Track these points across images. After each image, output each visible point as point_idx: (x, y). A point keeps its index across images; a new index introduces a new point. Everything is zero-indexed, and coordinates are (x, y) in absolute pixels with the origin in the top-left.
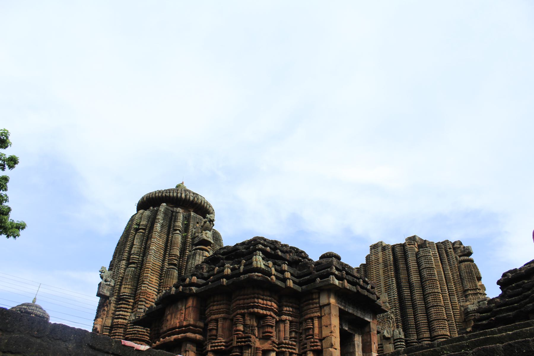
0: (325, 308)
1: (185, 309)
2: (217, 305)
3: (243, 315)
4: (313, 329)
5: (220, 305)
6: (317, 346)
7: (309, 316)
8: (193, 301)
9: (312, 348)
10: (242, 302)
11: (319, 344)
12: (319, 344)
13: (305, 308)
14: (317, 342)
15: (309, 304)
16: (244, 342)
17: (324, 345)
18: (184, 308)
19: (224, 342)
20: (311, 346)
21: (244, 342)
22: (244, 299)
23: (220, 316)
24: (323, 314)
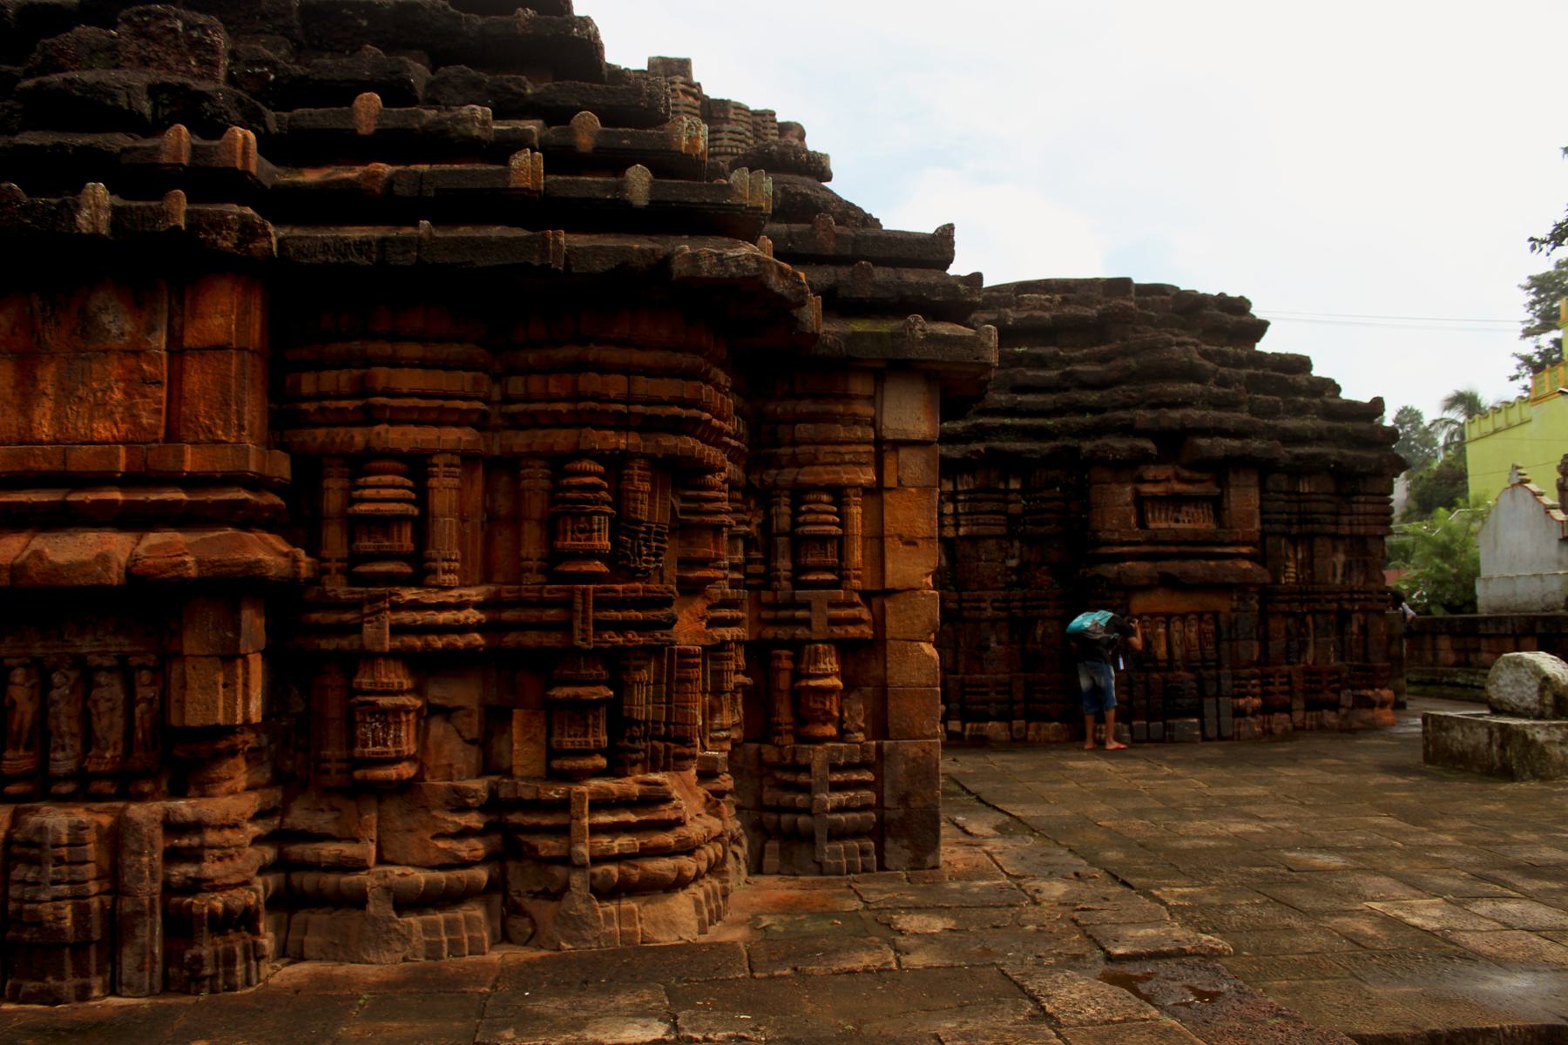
0: (904, 453)
1: (176, 349)
2: (424, 364)
3: (616, 463)
4: (841, 542)
5: (446, 365)
6: (857, 621)
7: (826, 476)
8: (244, 313)
9: (838, 631)
10: (616, 384)
11: (865, 614)
12: (865, 614)
13: (804, 430)
14: (853, 605)
15: (832, 418)
16: (643, 627)
17: (891, 622)
18: (160, 341)
19: (478, 606)
20: (834, 622)
21: (643, 627)
22: (629, 370)
23: (454, 436)
24: (890, 481)
